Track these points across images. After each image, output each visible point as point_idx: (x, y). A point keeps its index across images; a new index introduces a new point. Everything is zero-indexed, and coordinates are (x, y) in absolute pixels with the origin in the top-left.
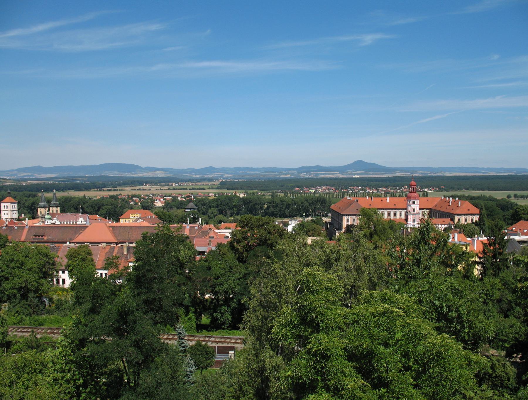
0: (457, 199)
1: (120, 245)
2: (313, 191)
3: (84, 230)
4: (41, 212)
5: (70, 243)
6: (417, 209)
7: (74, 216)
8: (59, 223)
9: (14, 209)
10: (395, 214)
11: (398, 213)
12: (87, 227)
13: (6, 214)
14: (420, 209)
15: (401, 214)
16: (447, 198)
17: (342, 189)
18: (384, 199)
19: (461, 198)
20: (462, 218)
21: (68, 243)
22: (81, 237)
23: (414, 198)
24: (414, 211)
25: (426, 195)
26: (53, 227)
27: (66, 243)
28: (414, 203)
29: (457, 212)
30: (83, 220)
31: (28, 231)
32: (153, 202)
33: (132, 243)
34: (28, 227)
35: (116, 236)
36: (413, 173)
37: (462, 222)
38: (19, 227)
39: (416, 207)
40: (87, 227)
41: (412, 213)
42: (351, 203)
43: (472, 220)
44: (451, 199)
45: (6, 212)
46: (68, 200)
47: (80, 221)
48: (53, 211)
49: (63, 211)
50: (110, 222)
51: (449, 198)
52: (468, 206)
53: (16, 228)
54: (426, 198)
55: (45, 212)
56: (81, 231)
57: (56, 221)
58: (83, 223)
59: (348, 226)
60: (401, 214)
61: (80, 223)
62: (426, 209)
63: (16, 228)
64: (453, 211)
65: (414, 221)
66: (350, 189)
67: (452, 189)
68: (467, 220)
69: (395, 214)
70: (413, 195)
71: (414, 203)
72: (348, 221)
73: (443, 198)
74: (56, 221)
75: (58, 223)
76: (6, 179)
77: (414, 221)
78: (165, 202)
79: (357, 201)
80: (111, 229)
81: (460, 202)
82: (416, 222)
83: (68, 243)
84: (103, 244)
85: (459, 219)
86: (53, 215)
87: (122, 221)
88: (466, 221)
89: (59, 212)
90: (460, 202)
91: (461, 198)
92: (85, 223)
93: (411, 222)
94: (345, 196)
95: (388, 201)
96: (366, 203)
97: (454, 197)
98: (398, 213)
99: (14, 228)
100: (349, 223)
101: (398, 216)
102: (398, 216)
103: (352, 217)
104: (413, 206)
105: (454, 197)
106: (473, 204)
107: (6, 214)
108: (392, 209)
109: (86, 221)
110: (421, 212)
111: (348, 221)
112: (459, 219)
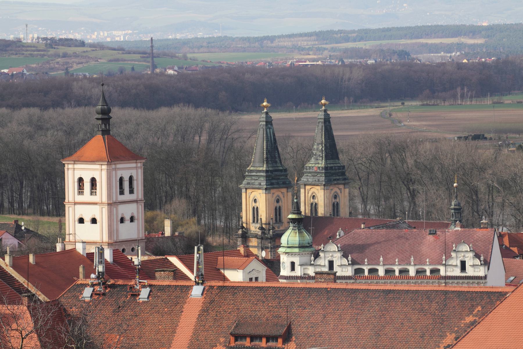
3: (483, 314)
8: (349, 272)
9: (127, 196)
12: (501, 296)
13: (87, 219)
31: (204, 311)
38: (162, 288)
40: (501, 296)
53: (144, 293)
55: (278, 212)
56: (469, 319)
58: (470, 272)
61: (457, 272)
63: (144, 293)
74: (338, 260)
76: (82, 44)
92: (481, 272)
99: (136, 295)
107: (87, 219)
109: (486, 263)
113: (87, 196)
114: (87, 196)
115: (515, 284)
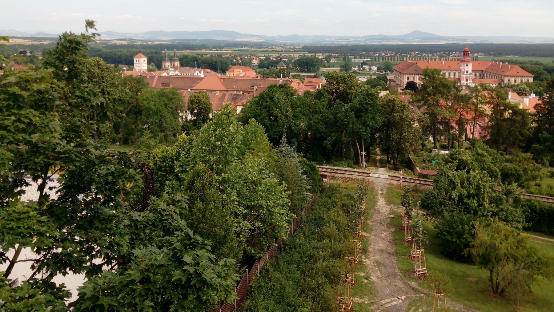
0: (507, 63)
1: (229, 93)
2: (378, 55)
4: (165, 66)
5: (191, 90)
6: (470, 71)
7: (192, 70)
8: (180, 74)
10: (449, 74)
11: (452, 74)
14: (472, 71)
15: (455, 74)
16: (498, 63)
17: (401, 54)
18: (440, 62)
19: (510, 62)
20: (512, 80)
21: (189, 90)
22: (199, 86)
23: (468, 61)
24: (467, 72)
25: (476, 59)
26: (176, 77)
27: (188, 89)
28: (467, 65)
29: (508, 74)
30: (198, 73)
32: (250, 60)
33: (239, 91)
34: (157, 77)
35: (225, 86)
36: (464, 41)
37: (512, 82)
39: (470, 69)
41: (465, 73)
42: (411, 65)
43: (522, 81)
44: (501, 63)
45: (138, 65)
46: (186, 57)
47: (196, 73)
48: (174, 65)
49: (182, 65)
50: (220, 75)
51: (499, 62)
52: (517, 68)
53: (148, 77)
54: (477, 62)
57: (177, 72)
59: (408, 82)
60: (455, 74)
62: (478, 71)
64: (504, 73)
65: (467, 80)
66: (409, 53)
67: (500, 54)
68: (517, 81)
69: (449, 74)
70: (466, 59)
71: (467, 65)
72: (408, 79)
73: (493, 62)
75: (179, 74)
77: (467, 80)
78: (260, 61)
79: (417, 63)
80: (222, 80)
81: (510, 66)
82: (469, 81)
83: (189, 90)
84: (217, 92)
85: (509, 80)
86: (175, 68)
87: (228, 74)
88: (515, 81)
89: (179, 66)
90: (510, 66)
91: (510, 62)
93: (465, 81)
94: (405, 59)
95: (443, 64)
96: (423, 65)
97: (504, 62)
98: (452, 74)
100: (410, 80)
101: (452, 76)
102: (452, 76)
103: (412, 75)
104: (466, 68)
105: (504, 62)
106: (522, 68)
108: (447, 70)
110: (473, 73)
111: (408, 79)
112: (509, 80)
113: (138, 63)
114: (138, 63)
115: (205, 77)
